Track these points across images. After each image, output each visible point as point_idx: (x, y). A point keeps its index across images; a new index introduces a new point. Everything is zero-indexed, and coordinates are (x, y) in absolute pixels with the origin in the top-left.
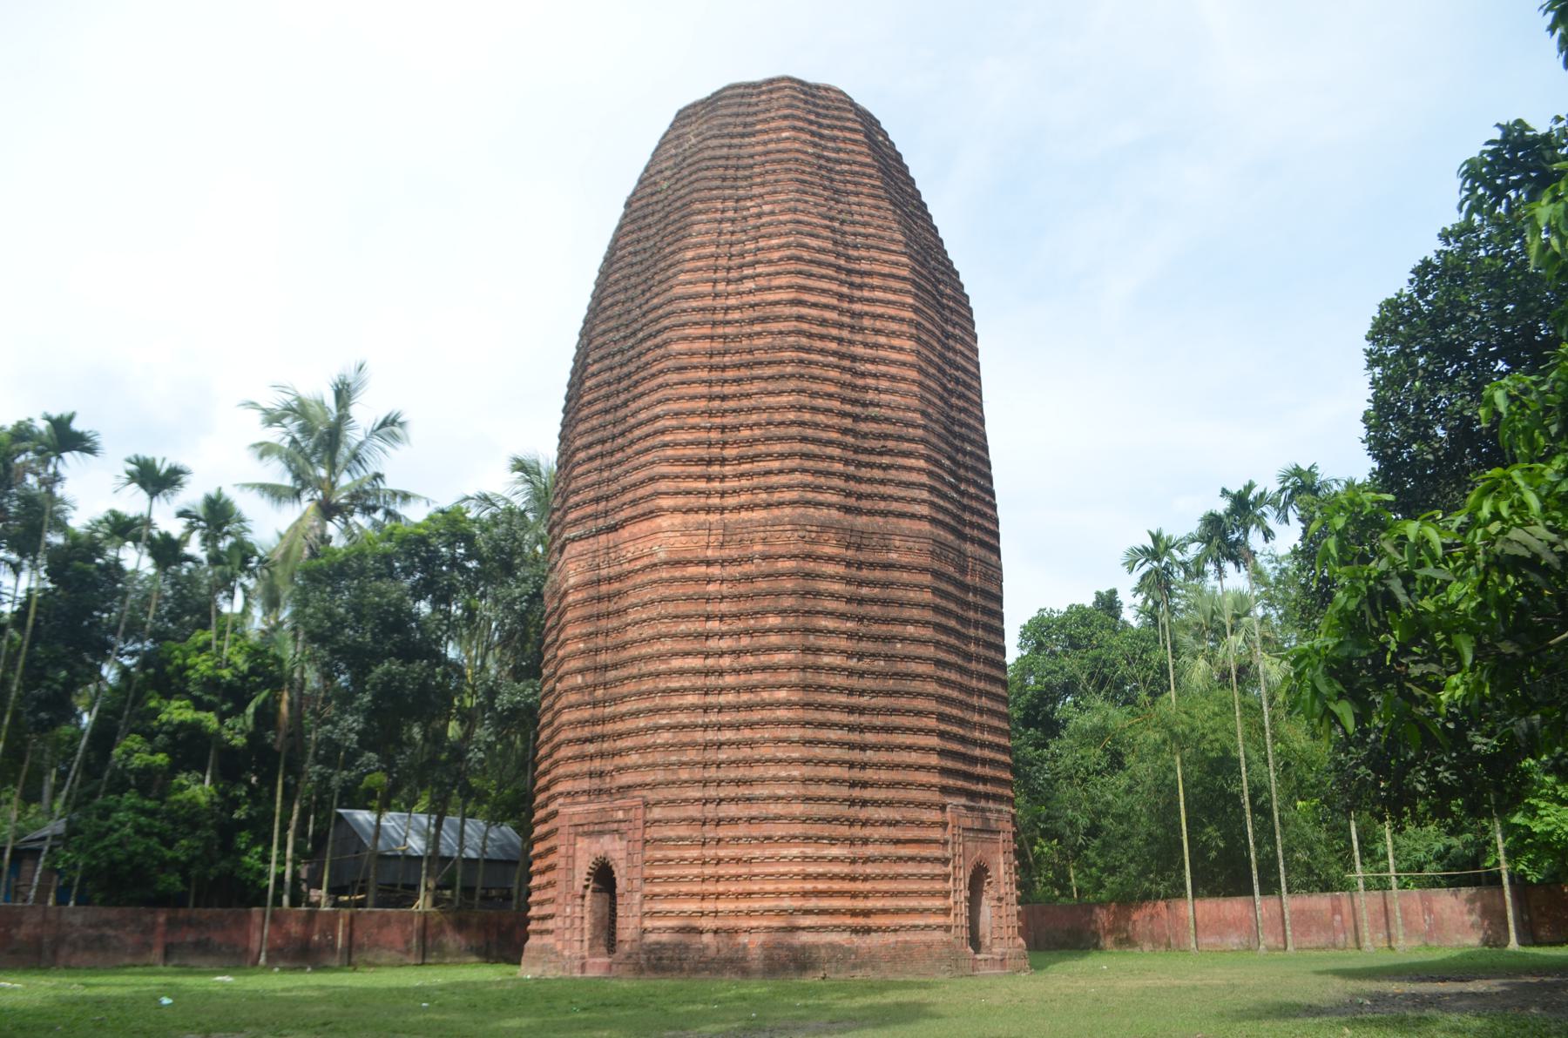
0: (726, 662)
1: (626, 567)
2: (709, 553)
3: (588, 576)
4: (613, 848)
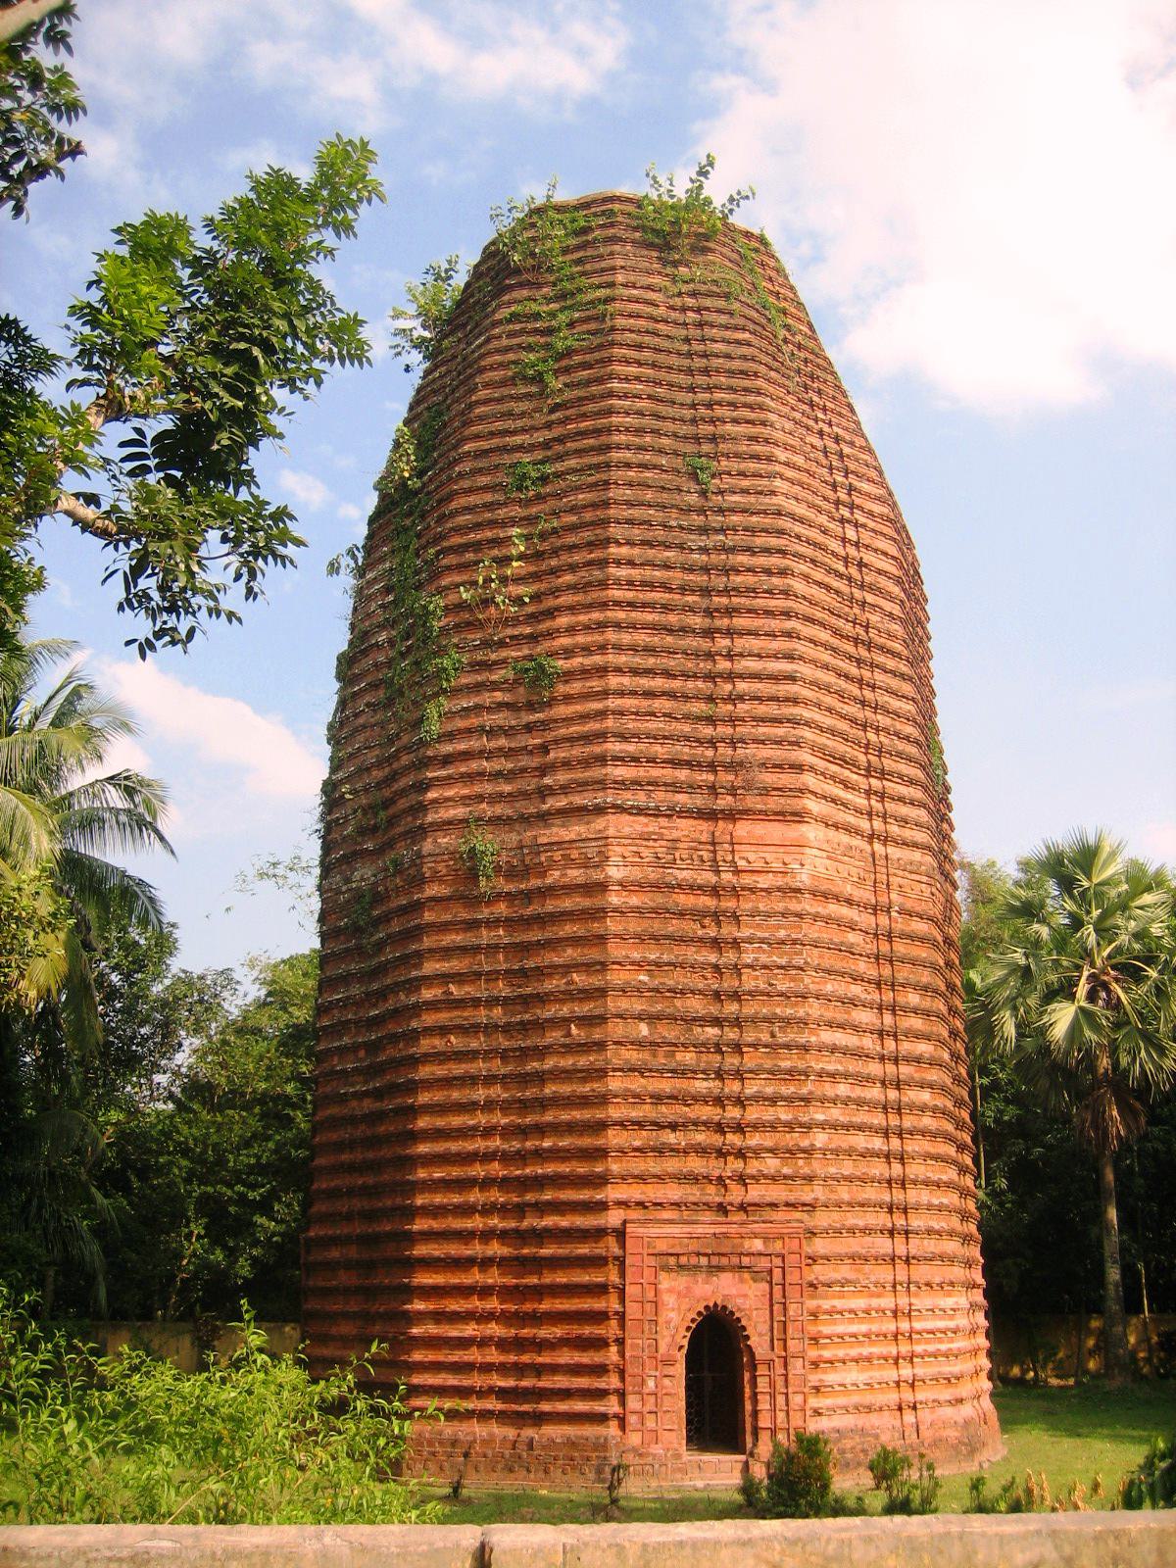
0: (869, 1043)
1: (727, 877)
2: (848, 889)
3: (653, 875)
4: (744, 1297)
